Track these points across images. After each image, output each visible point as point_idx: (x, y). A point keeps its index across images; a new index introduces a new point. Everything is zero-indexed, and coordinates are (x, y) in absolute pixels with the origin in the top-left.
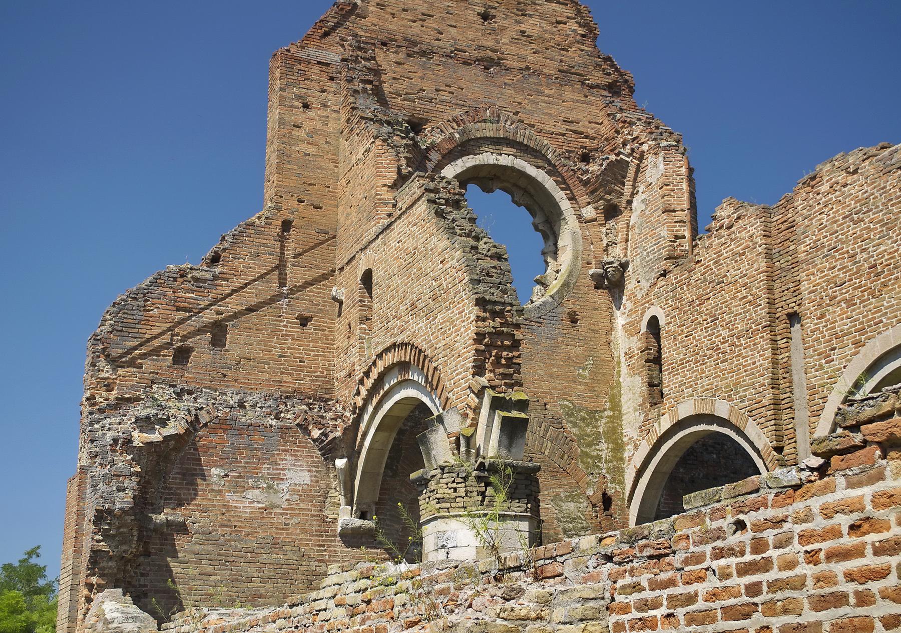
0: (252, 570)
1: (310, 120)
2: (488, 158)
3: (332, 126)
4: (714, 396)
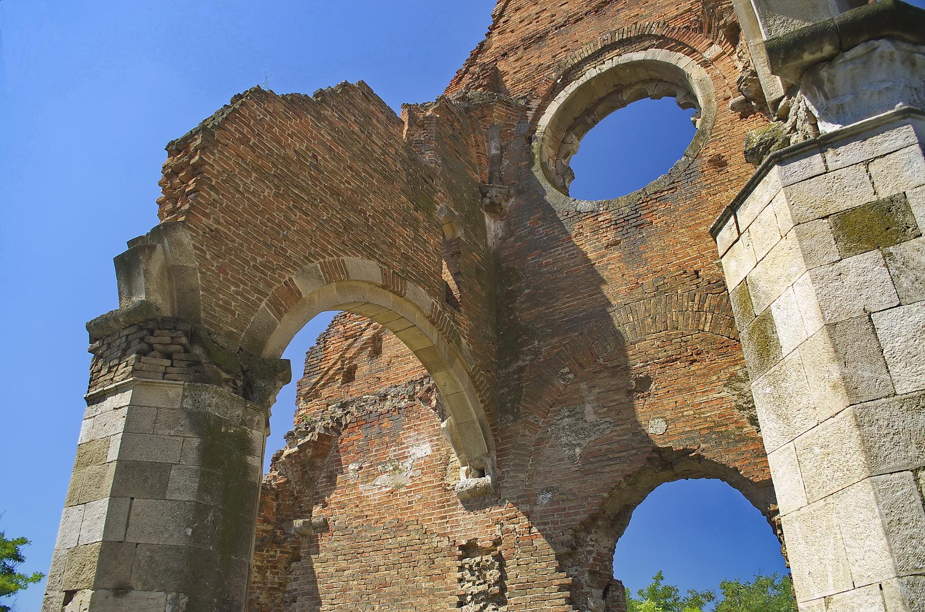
0: (379, 559)
2: (591, 72)
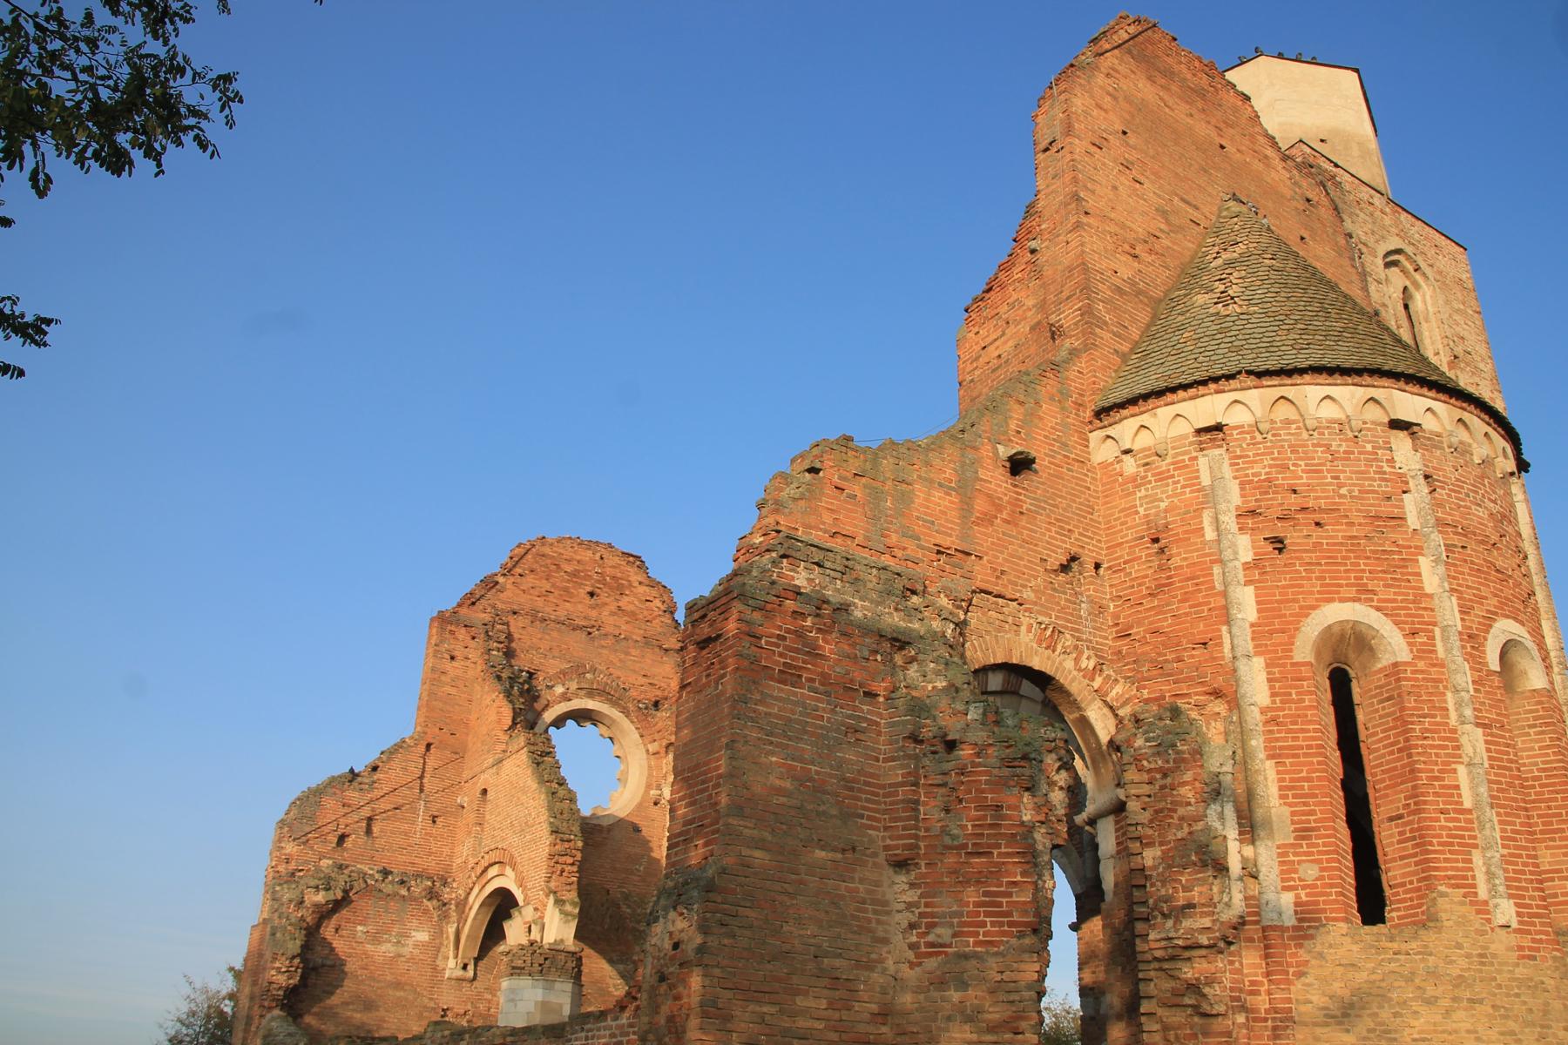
3: (471, 673)
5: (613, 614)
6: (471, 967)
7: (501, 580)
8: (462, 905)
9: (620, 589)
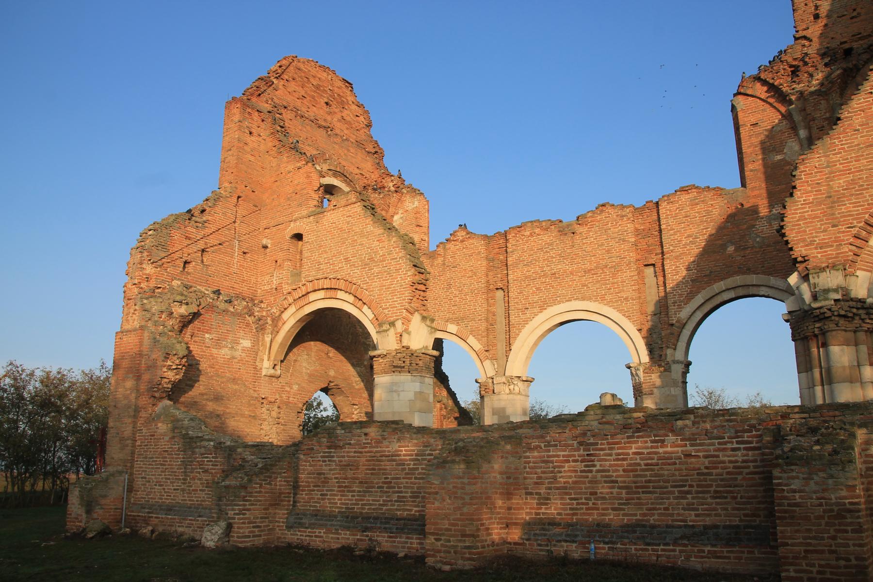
1: (252, 140)
3: (262, 148)
4: (447, 321)
5: (339, 121)
6: (278, 367)
7: (275, 81)
8: (277, 321)
9: (343, 105)
